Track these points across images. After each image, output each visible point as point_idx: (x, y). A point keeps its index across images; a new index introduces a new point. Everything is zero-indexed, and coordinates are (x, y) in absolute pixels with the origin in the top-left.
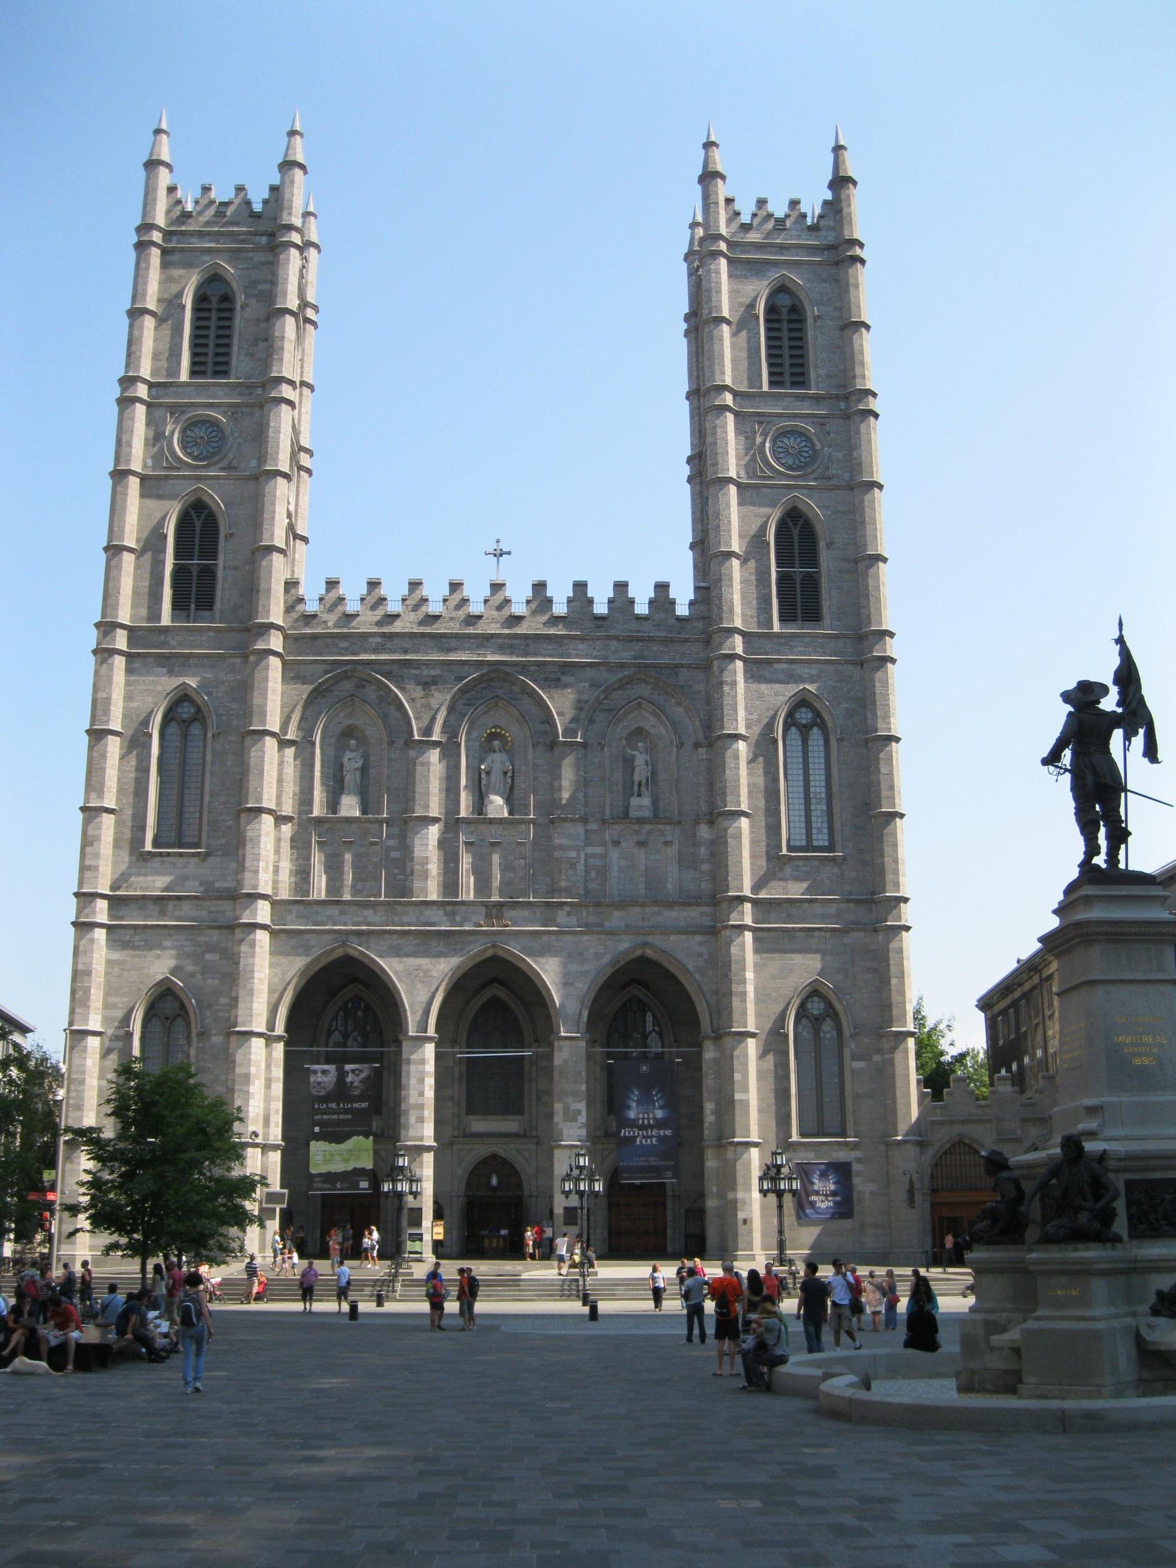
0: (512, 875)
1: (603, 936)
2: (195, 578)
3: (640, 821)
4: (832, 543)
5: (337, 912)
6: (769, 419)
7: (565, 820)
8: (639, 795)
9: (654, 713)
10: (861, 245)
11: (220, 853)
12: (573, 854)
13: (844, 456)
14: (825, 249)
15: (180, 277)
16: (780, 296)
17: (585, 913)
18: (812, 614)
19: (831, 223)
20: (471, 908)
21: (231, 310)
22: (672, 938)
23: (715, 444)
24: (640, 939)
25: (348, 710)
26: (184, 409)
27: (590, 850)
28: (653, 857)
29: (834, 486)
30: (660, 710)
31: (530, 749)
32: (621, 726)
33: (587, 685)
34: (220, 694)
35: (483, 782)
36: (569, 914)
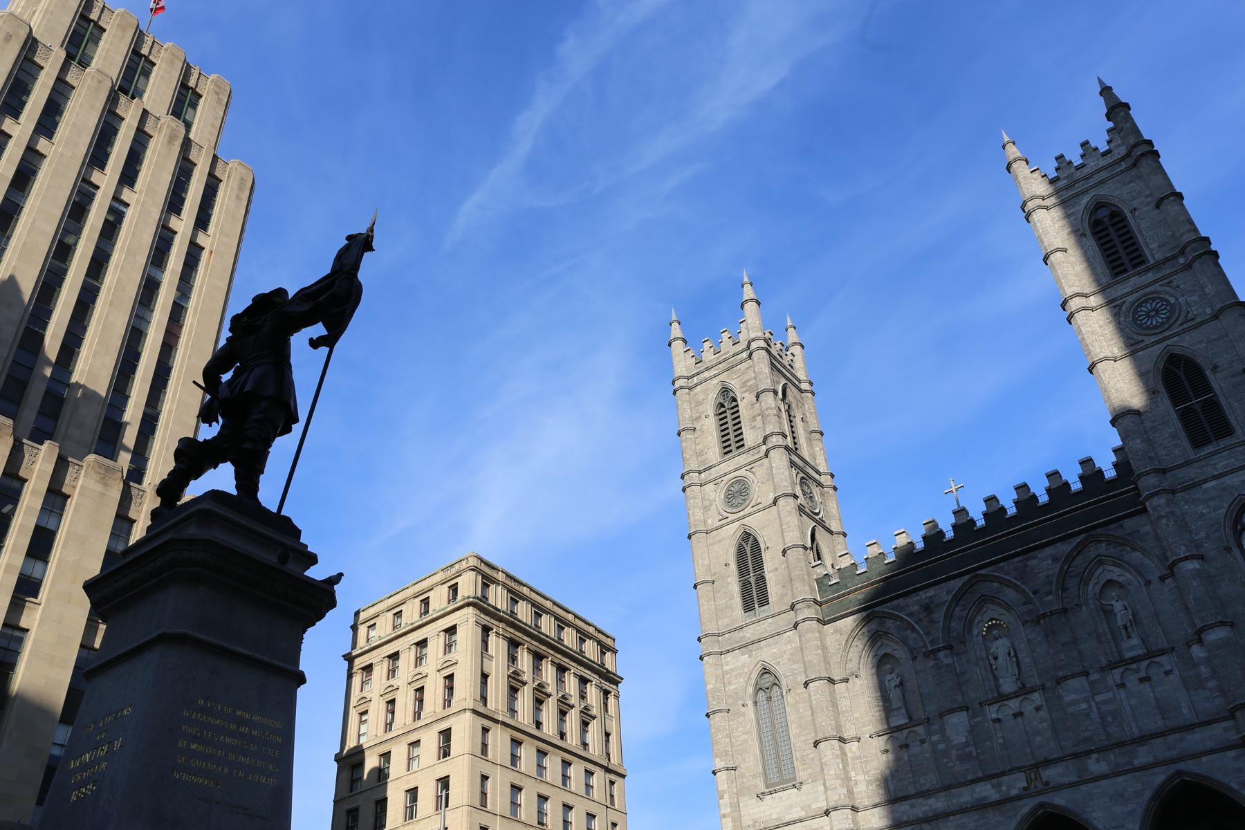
0: (1039, 739)
1: (1136, 774)
2: (753, 586)
3: (1135, 660)
4: (1216, 367)
5: (907, 807)
6: (1123, 300)
7: (1066, 678)
8: (1129, 637)
9: (1115, 564)
10: (1150, 143)
11: (810, 781)
12: (1084, 706)
13: (1199, 296)
14: (1122, 161)
15: (703, 400)
16: (1099, 211)
17: (1112, 756)
18: (1223, 429)
19: (1120, 142)
20: (1013, 776)
21: (737, 406)
22: (1204, 759)
23: (1083, 339)
24: (1173, 768)
25: (879, 643)
26: (722, 479)
27: (1099, 698)
28: (1159, 689)
29: (1198, 323)
30: (1120, 560)
31: (1022, 629)
32: (1091, 584)
33: (1050, 561)
34: (785, 661)
35: (994, 667)
36: (1098, 761)
